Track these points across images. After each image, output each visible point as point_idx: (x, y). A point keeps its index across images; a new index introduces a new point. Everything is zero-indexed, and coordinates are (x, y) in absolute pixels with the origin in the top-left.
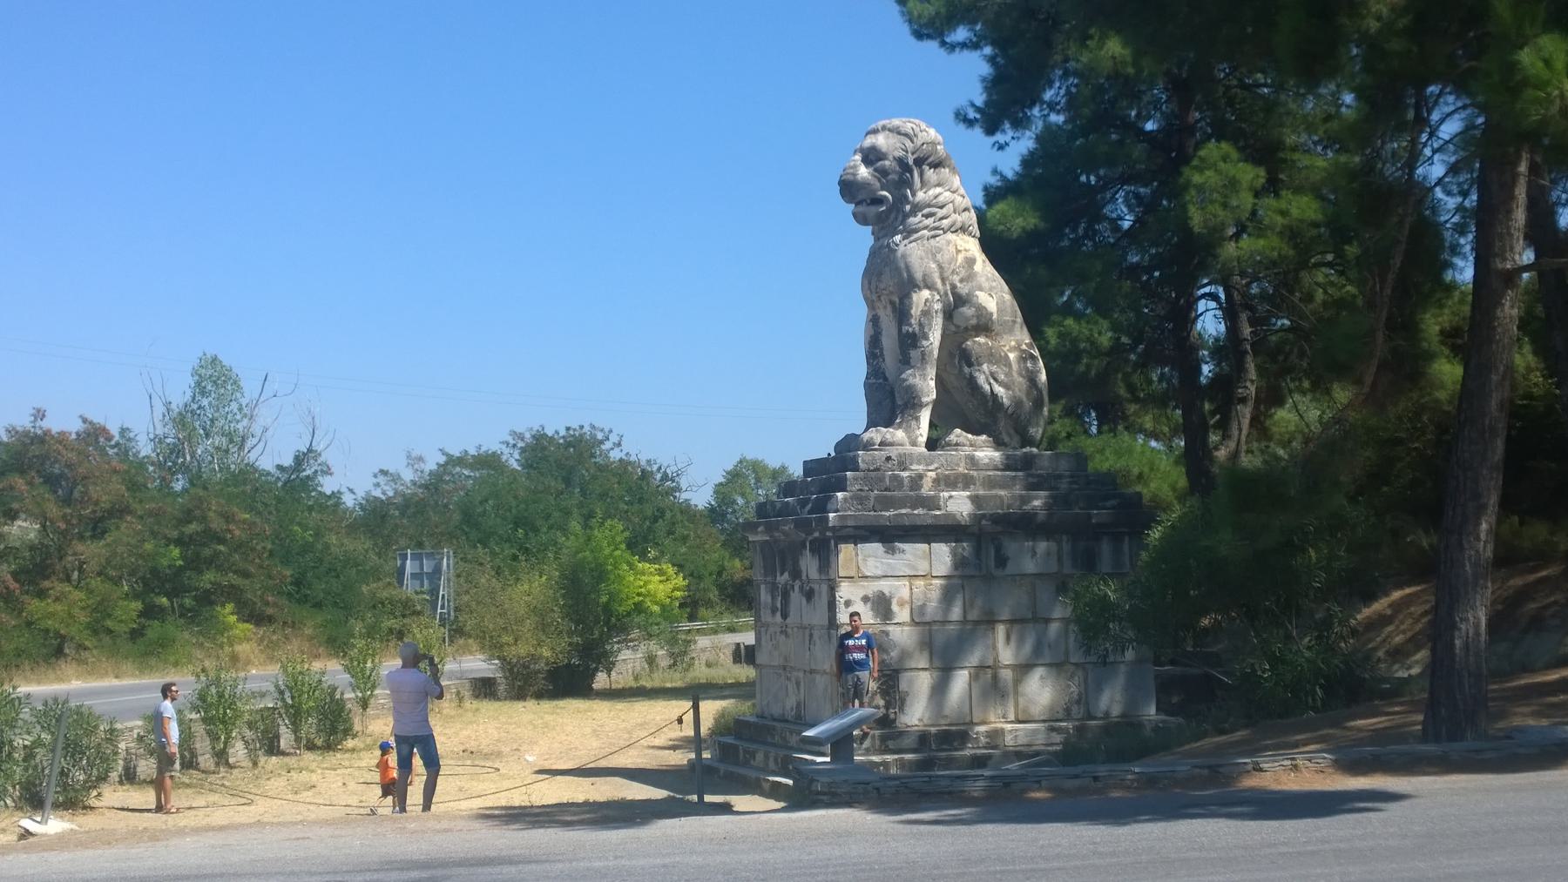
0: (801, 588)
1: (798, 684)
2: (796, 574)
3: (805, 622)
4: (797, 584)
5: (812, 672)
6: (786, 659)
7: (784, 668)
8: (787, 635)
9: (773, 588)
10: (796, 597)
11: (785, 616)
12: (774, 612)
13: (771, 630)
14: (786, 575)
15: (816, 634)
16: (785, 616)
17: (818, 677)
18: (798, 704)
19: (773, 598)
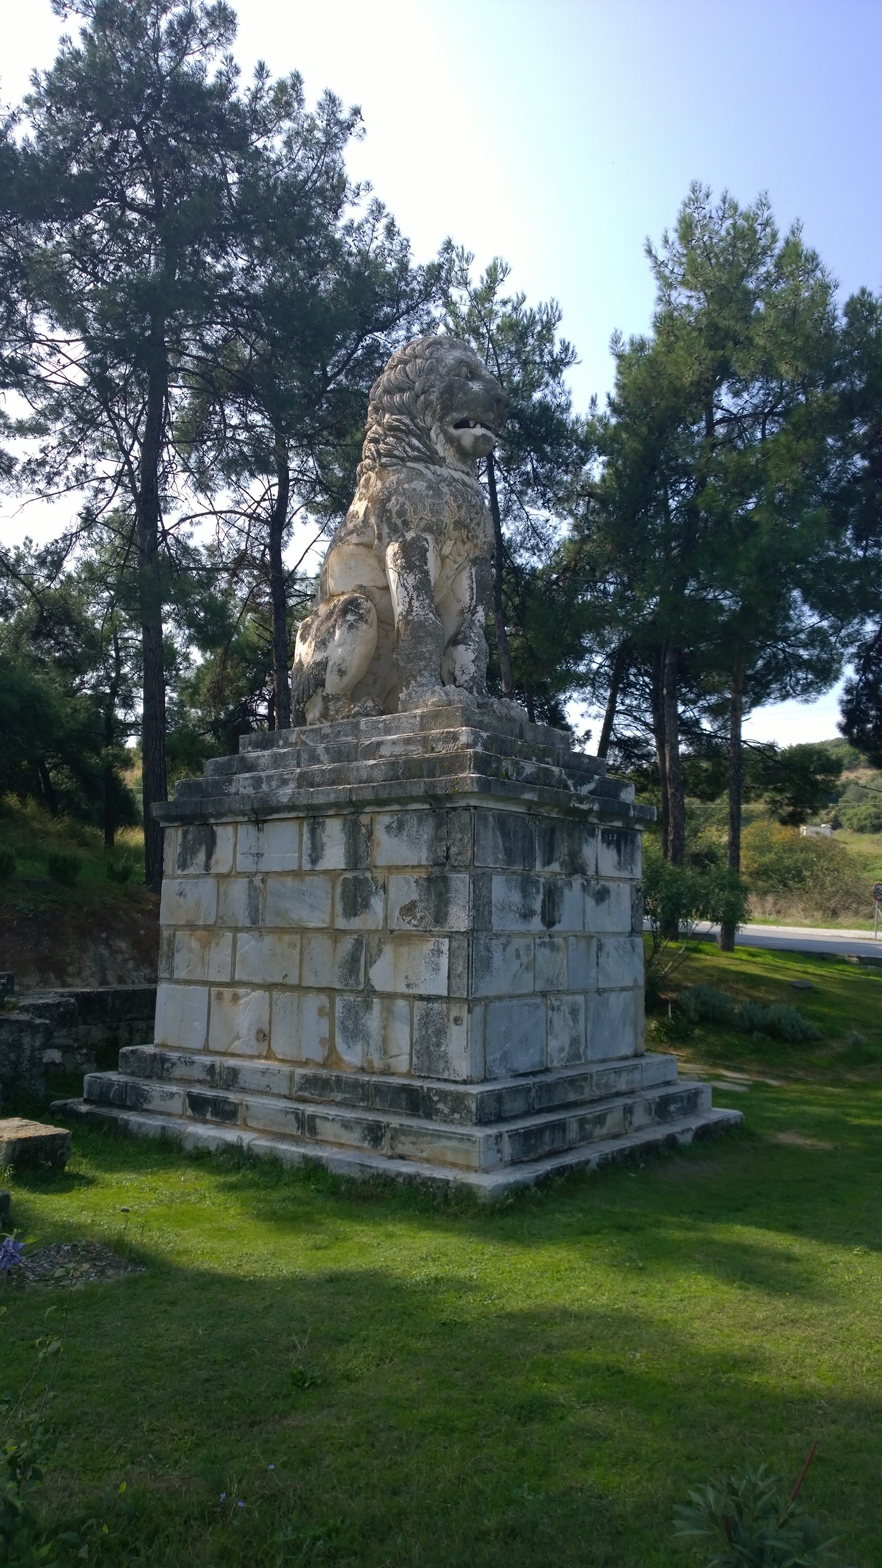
0: (584, 888)
1: (574, 1012)
2: (575, 867)
3: (591, 928)
4: (577, 881)
5: (600, 992)
6: (550, 981)
7: (544, 994)
8: (553, 947)
9: (526, 884)
10: (573, 896)
11: (549, 921)
12: (527, 915)
13: (517, 942)
14: (555, 867)
15: (610, 944)
16: (549, 921)
17: (613, 998)
18: (574, 1041)
19: (525, 893)
